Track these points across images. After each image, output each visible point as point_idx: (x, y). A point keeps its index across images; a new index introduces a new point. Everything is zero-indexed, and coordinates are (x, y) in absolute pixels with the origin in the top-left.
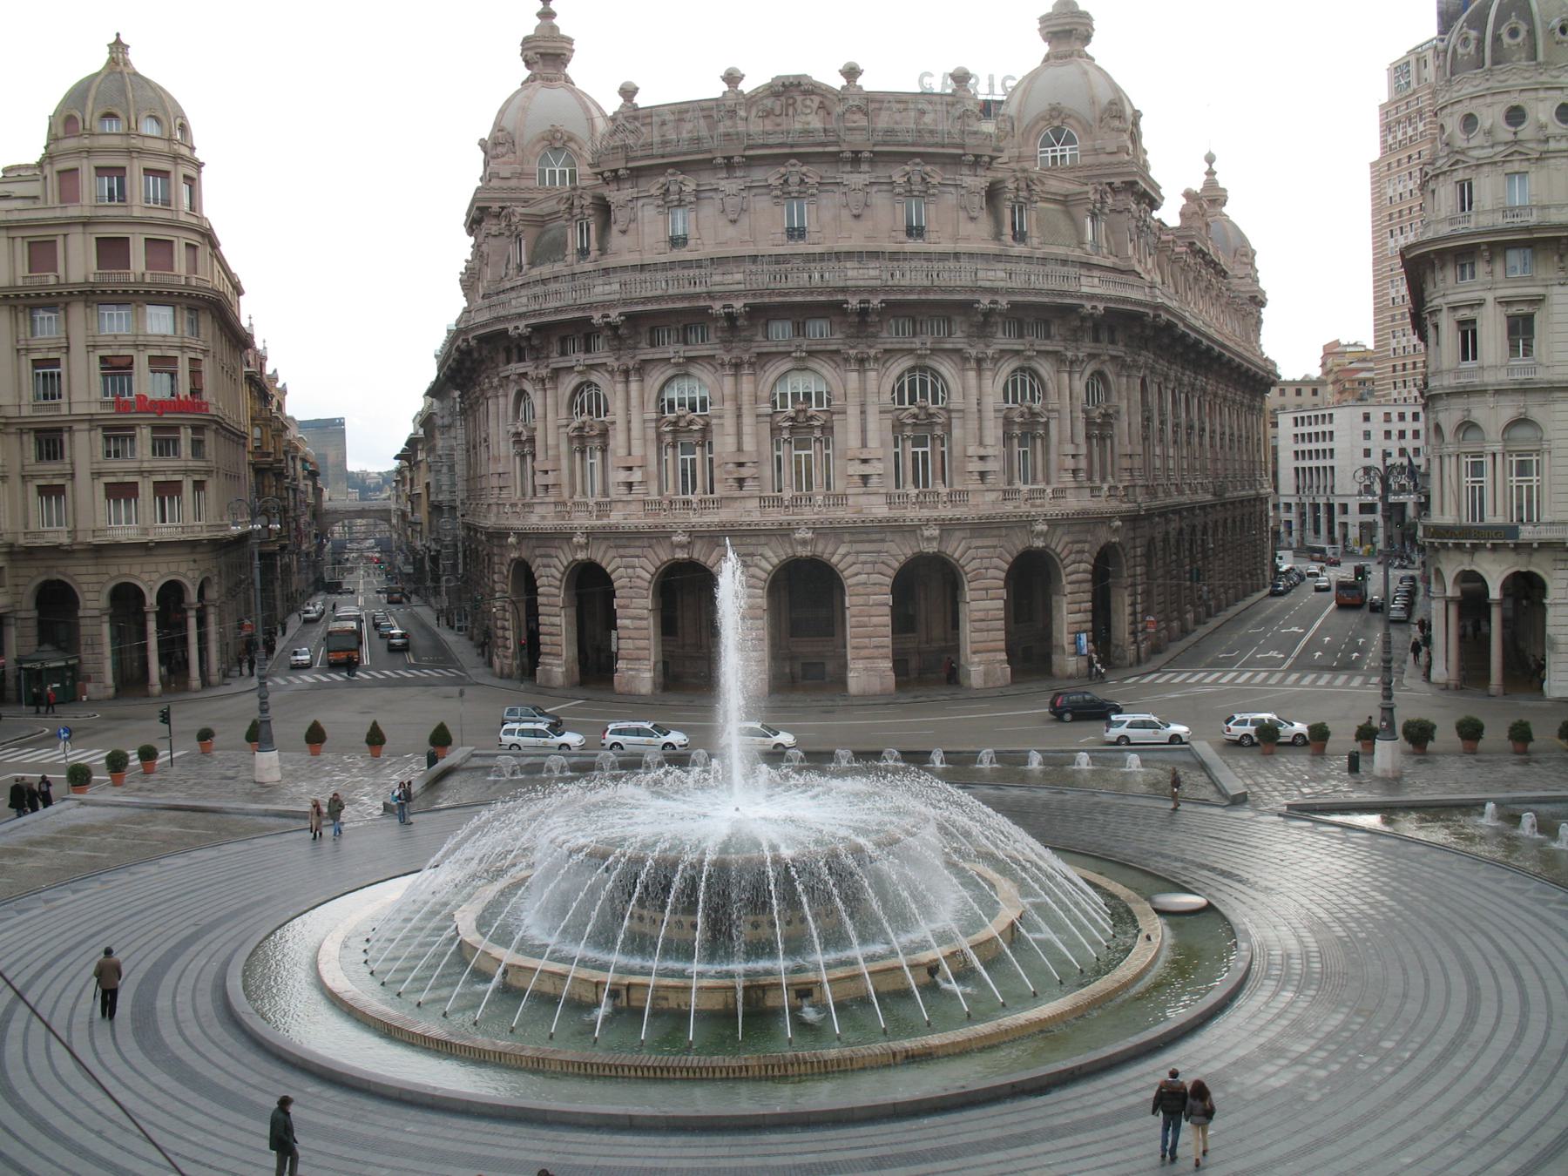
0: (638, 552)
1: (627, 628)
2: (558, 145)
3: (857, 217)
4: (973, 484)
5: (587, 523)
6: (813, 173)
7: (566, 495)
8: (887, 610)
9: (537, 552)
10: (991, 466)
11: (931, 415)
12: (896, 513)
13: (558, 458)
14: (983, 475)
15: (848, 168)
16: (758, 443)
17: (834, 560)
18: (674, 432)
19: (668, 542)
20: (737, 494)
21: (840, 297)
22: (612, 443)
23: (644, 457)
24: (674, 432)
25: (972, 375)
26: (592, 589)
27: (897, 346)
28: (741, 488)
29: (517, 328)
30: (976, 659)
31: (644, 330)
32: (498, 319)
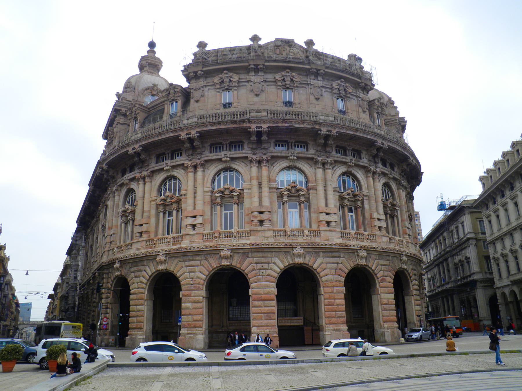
0: (198, 263)
1: (188, 308)
2: (155, 93)
3: (317, 99)
4: (377, 232)
5: (167, 248)
6: (297, 78)
7: (152, 236)
8: (343, 296)
9: (132, 270)
10: (383, 224)
11: (355, 196)
12: (347, 242)
13: (149, 217)
14: (380, 228)
15: (313, 77)
16: (271, 203)
17: (315, 266)
18: (222, 197)
19: (217, 256)
20: (260, 228)
21: (317, 127)
22: (183, 206)
23: (203, 211)
24: (222, 197)
25: (371, 179)
26: (166, 290)
27: (340, 159)
28: (261, 225)
29: (134, 149)
30: (386, 325)
31: (207, 145)
32: (123, 147)
